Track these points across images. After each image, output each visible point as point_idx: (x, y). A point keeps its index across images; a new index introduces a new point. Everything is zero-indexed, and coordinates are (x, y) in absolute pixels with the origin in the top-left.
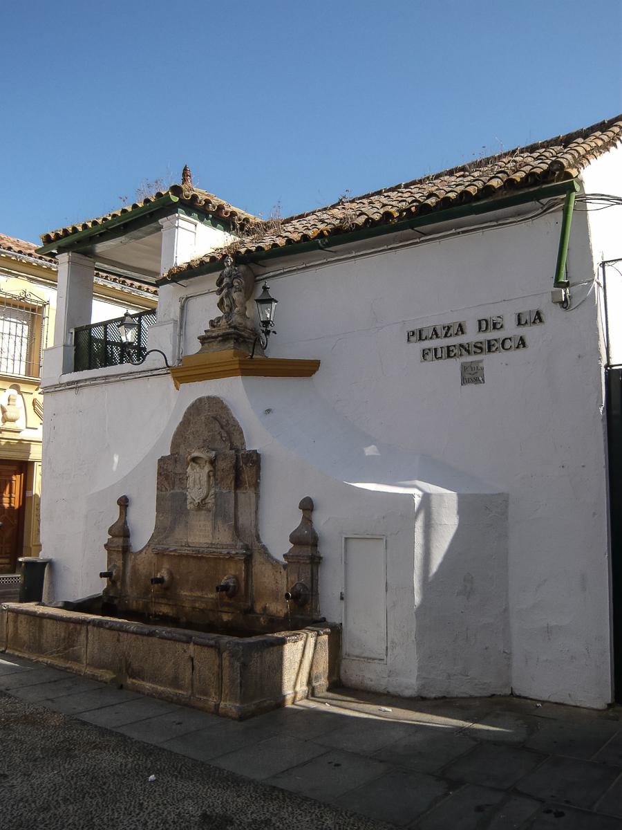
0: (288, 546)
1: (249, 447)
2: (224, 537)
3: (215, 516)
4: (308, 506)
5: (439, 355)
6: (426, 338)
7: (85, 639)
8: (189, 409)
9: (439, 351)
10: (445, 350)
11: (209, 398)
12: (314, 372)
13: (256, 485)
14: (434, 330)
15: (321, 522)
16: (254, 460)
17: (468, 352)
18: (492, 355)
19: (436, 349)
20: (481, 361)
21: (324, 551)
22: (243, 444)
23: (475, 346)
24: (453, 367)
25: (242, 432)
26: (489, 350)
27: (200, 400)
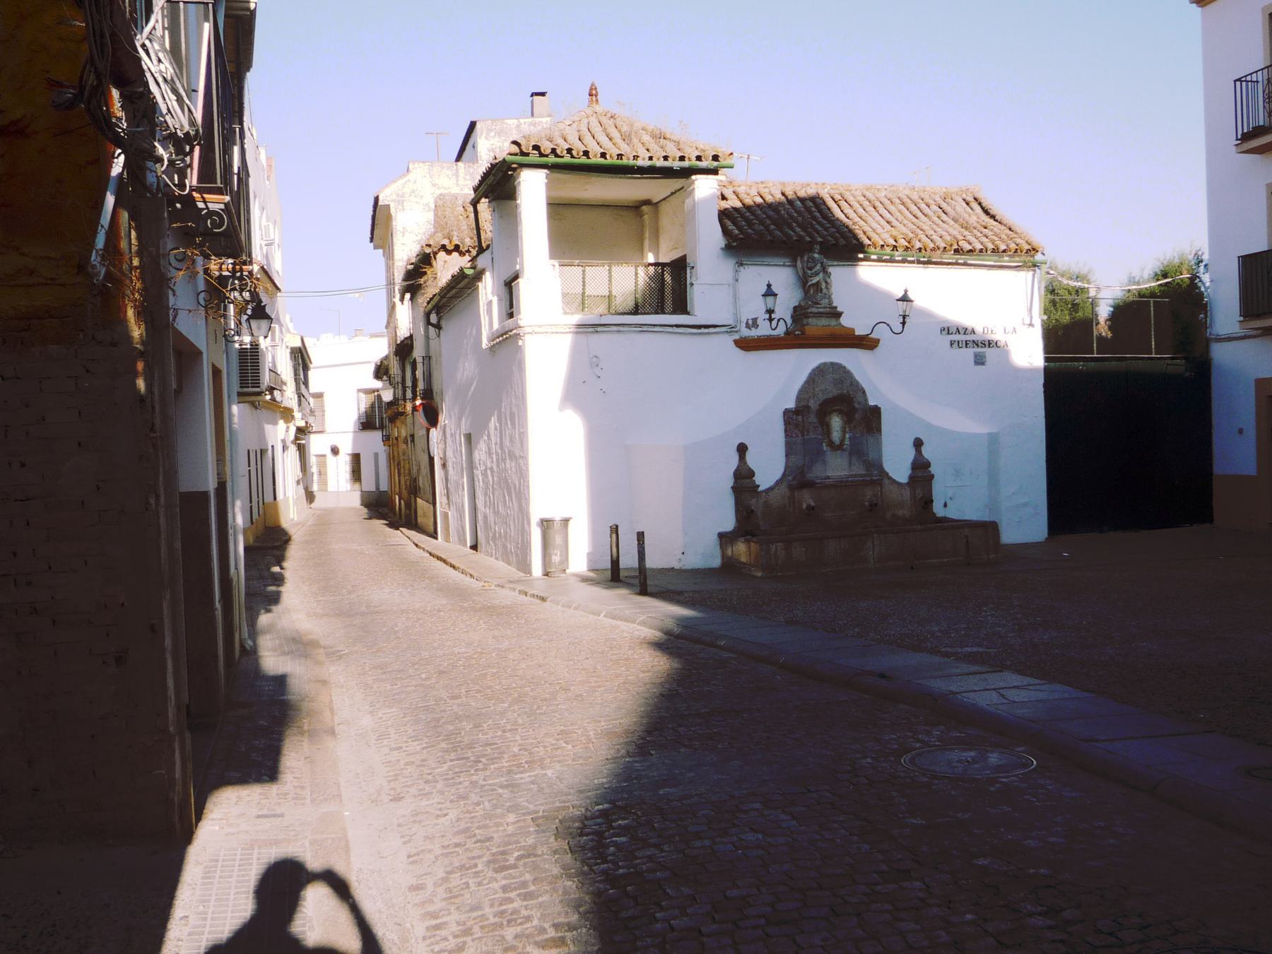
0: (908, 472)
1: (872, 403)
2: (859, 469)
3: (851, 454)
4: (918, 444)
5: (960, 346)
6: (952, 334)
7: (871, 545)
8: (814, 370)
9: (960, 342)
10: (964, 342)
11: (832, 364)
12: (876, 347)
13: (879, 430)
14: (958, 329)
15: (926, 452)
16: (876, 411)
17: (977, 345)
18: (990, 349)
19: (958, 342)
20: (984, 352)
21: (933, 469)
22: (866, 400)
23: (982, 343)
24: (969, 353)
25: (864, 392)
26: (989, 347)
27: (825, 364)
